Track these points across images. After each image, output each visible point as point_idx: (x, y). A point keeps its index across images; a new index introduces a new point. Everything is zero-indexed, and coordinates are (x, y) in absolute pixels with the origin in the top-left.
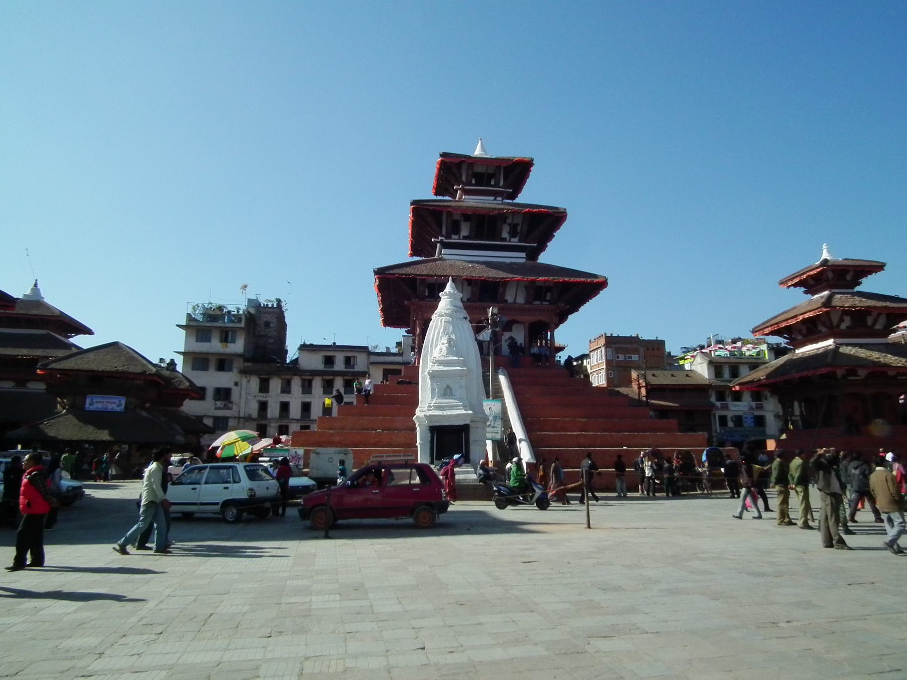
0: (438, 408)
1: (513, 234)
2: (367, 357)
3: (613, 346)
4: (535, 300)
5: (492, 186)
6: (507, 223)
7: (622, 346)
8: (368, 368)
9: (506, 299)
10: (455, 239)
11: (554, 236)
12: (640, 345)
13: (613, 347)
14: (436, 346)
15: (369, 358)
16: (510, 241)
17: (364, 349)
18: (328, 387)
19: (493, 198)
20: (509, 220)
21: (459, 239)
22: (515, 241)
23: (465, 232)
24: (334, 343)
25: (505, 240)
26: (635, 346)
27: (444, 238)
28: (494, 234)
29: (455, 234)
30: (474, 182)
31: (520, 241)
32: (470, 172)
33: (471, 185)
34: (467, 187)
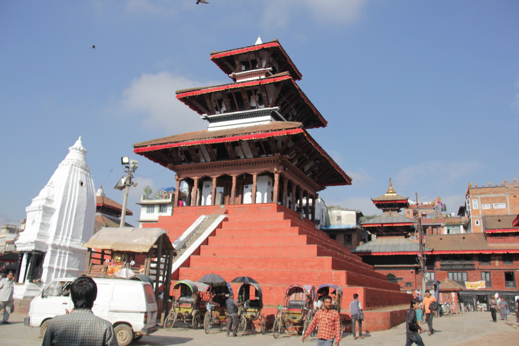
3: (479, 196)
5: (257, 68)
6: (257, 94)
7: (488, 196)
9: (239, 155)
10: (218, 115)
12: (506, 194)
13: (479, 199)
16: (258, 108)
20: (258, 92)
21: (221, 113)
22: (262, 108)
23: (224, 109)
26: (502, 195)
27: (206, 115)
30: (244, 68)
31: (266, 107)
33: (241, 70)
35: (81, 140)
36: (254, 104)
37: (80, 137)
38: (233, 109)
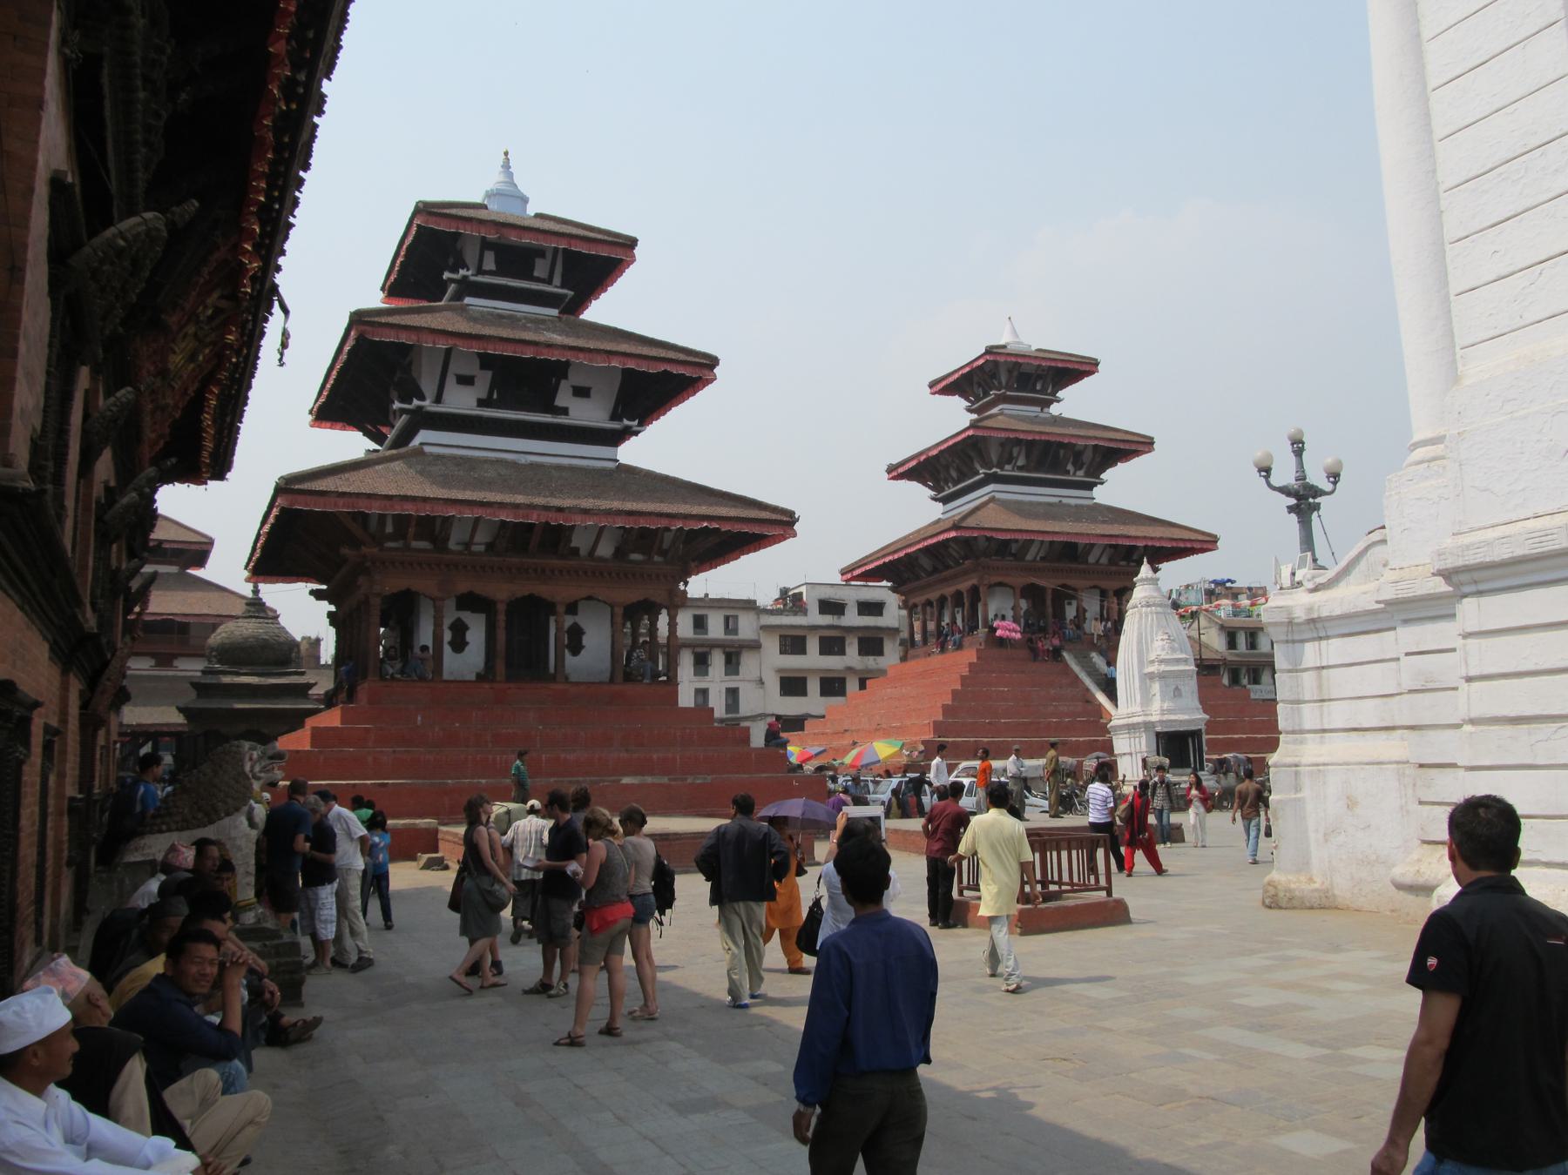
0: (1170, 711)
1: (1078, 466)
2: (756, 617)
4: (1123, 559)
8: (759, 634)
10: (1008, 471)
11: (1116, 465)
14: (1152, 641)
15: (759, 618)
16: (1074, 474)
17: (749, 605)
18: (701, 663)
19: (1038, 409)
21: (1013, 470)
24: (707, 595)
25: (1068, 472)
28: (1057, 466)
29: (1009, 462)
30: (1015, 386)
31: (1087, 474)
32: (1015, 373)
34: (1008, 393)
35: (1149, 562)
36: (1070, 467)
37: (1145, 560)
38: (1037, 470)
